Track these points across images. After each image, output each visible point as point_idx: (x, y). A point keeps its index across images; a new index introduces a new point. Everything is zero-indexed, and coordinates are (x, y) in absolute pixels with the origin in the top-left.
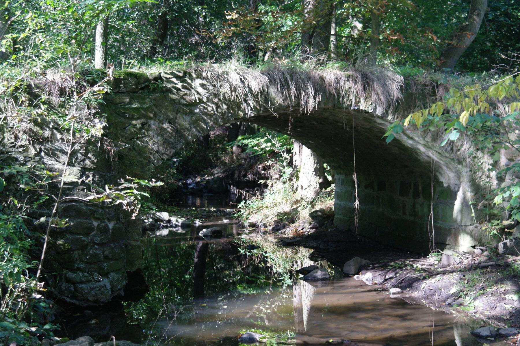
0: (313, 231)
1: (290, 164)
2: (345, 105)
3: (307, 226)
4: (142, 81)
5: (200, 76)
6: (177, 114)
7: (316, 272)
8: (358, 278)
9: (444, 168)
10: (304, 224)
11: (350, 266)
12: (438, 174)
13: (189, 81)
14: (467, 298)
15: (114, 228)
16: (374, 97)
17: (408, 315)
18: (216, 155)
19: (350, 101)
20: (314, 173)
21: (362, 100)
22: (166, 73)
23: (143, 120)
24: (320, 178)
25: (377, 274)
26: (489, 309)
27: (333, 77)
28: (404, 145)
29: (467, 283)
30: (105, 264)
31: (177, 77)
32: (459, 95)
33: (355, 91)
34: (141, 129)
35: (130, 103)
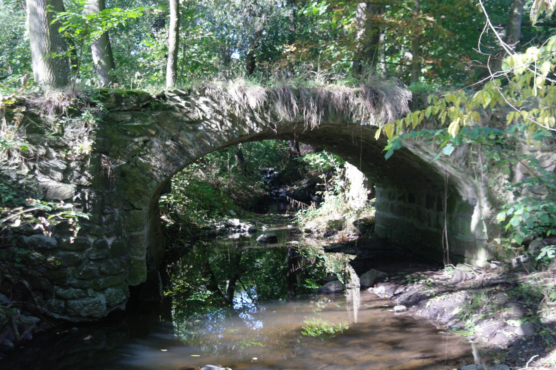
0: (357, 237)
1: (343, 178)
2: (354, 121)
3: (352, 233)
4: (143, 99)
5: (203, 94)
6: (180, 131)
7: (331, 285)
8: (372, 290)
9: (462, 182)
10: (349, 233)
11: (366, 278)
12: (457, 188)
13: (193, 99)
14: (469, 321)
15: (113, 245)
16: (383, 113)
17: (399, 341)
18: (304, 169)
19: (359, 118)
20: (363, 185)
21: (372, 116)
22: (170, 92)
23: (146, 138)
24: (368, 190)
25: (388, 287)
26: (488, 336)
27: (341, 93)
28: (422, 160)
29: (471, 304)
30: (101, 280)
31: (180, 95)
32: (441, 103)
33: (364, 107)
34: (143, 146)
35: (132, 121)
